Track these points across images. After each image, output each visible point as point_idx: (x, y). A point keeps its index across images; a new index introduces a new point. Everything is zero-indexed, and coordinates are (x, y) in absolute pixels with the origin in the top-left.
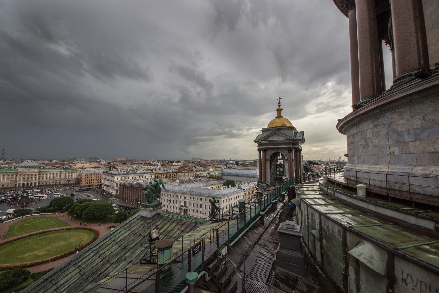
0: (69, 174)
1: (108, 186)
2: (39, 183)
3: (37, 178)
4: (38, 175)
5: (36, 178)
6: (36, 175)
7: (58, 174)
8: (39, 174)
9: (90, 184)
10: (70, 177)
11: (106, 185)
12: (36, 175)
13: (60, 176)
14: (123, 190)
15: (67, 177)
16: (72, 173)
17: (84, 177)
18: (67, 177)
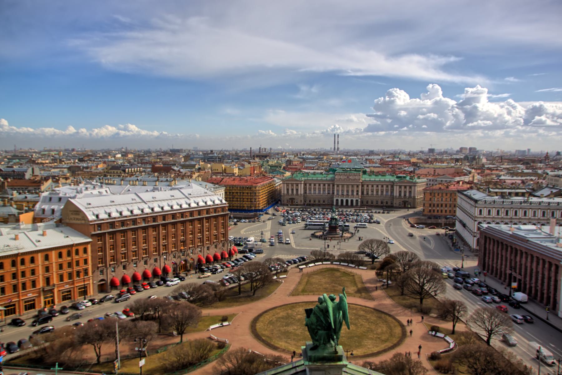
0: (405, 187)
1: (464, 225)
2: (362, 202)
3: (360, 194)
4: (360, 187)
5: (357, 191)
7: (390, 187)
9: (436, 213)
10: (407, 195)
11: (461, 222)
12: (358, 186)
14: (485, 244)
15: (403, 194)
16: (410, 187)
18: (403, 194)
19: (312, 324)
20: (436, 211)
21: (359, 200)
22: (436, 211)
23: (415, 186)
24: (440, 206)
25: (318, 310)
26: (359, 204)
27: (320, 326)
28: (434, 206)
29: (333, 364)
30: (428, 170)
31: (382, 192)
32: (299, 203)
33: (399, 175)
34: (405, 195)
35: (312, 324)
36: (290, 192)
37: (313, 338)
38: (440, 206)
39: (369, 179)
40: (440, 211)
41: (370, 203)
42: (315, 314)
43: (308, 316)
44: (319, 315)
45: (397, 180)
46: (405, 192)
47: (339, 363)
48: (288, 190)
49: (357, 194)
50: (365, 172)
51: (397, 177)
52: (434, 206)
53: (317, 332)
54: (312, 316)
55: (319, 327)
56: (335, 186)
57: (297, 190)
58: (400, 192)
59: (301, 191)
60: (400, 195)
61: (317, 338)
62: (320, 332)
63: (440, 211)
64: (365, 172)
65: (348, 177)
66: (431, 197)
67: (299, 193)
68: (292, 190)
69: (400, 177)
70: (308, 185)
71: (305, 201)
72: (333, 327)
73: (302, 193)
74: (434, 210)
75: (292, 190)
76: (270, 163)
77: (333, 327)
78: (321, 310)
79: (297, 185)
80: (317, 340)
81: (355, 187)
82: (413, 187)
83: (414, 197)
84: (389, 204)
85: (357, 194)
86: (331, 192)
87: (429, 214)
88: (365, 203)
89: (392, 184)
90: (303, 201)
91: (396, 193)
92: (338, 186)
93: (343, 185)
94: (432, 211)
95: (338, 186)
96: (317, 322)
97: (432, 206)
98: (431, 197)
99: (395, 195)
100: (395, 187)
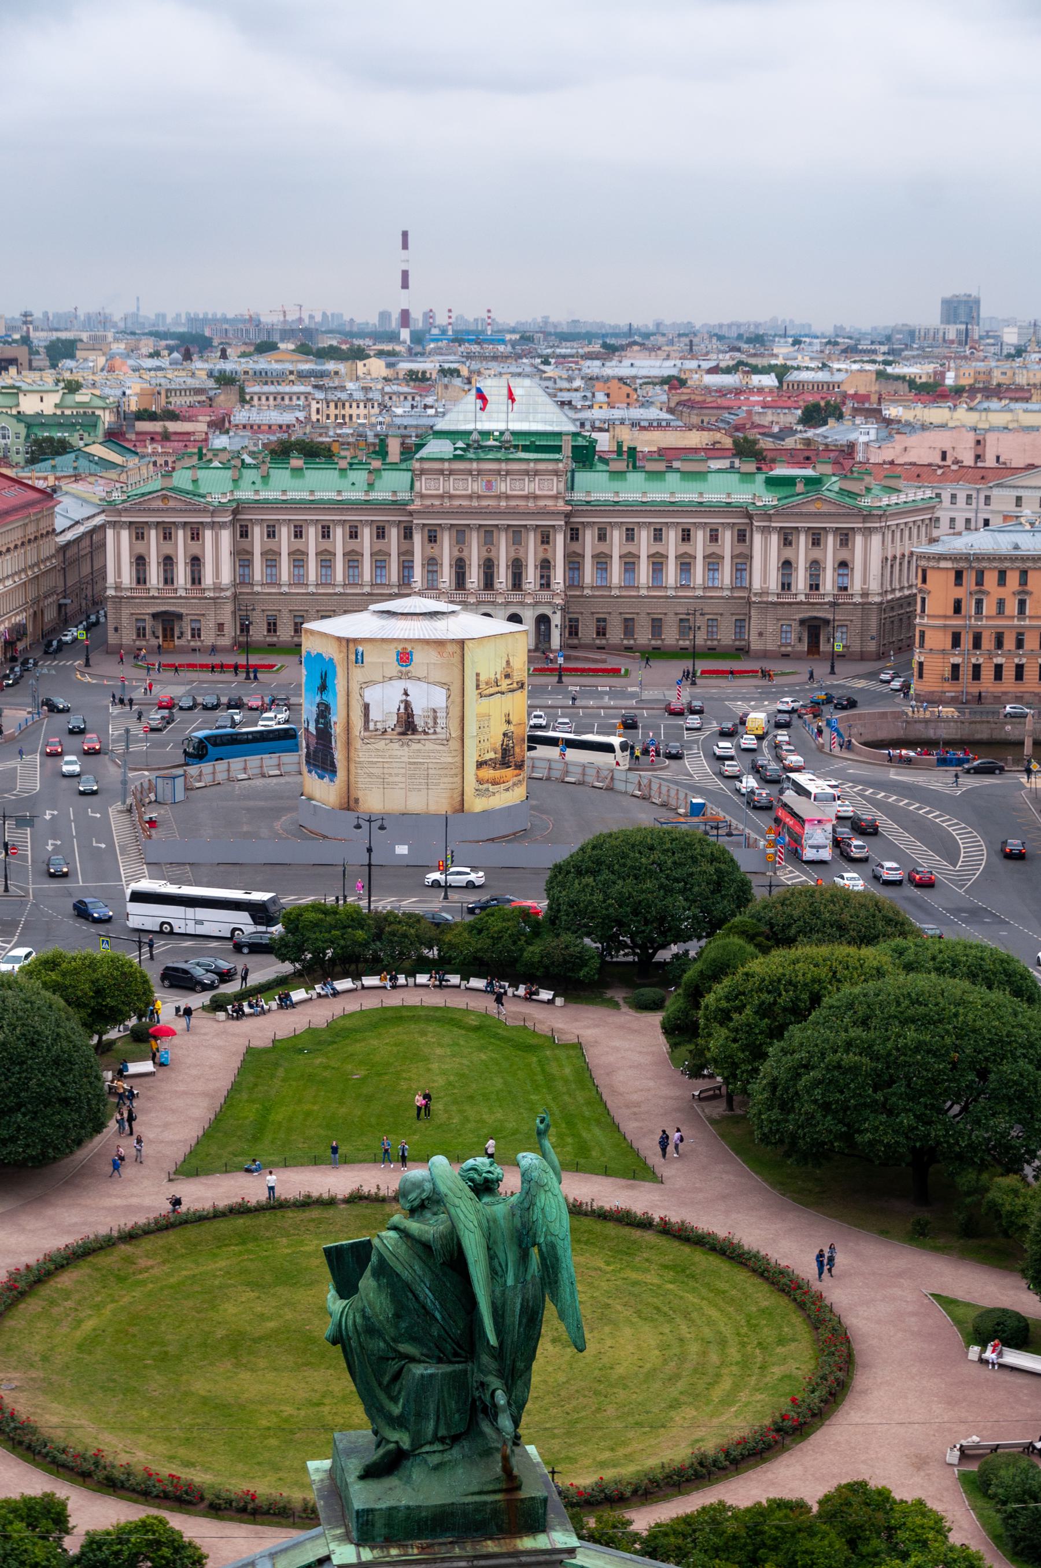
2: (572, 629)
3: (558, 577)
4: (560, 539)
5: (545, 565)
6: (546, 539)
7: (727, 538)
8: (574, 534)
10: (829, 583)
12: (546, 539)
13: (743, 562)
15: (801, 581)
16: (845, 538)
17: (940, 594)
18: (801, 581)
19: (371, 1330)
20: (988, 673)
21: (556, 619)
22: (988, 673)
23: (868, 532)
24: (1009, 643)
25: (402, 1250)
26: (556, 641)
27: (414, 1339)
28: (977, 644)
29: (491, 1546)
30: (942, 440)
31: (685, 564)
32: (208, 638)
33: (781, 471)
34: (815, 587)
35: (371, 1330)
36: (154, 574)
37: (374, 1409)
38: (1009, 643)
39: (610, 497)
40: (1009, 673)
41: (615, 635)
42: (384, 1270)
43: (346, 1289)
44: (405, 1275)
45: (768, 499)
46: (815, 567)
47: (527, 1543)
48: (140, 561)
49: (546, 584)
50: (585, 456)
51: (773, 482)
52: (977, 644)
53: (397, 1376)
54: (367, 1283)
55: (405, 1348)
56: (417, 538)
57: (196, 561)
58: (787, 565)
59: (220, 569)
60: (786, 586)
61: (396, 1410)
62: (419, 1370)
63: (1009, 673)
64: (585, 456)
65: (489, 485)
66: (960, 593)
67: (208, 580)
68: (168, 561)
69: (789, 482)
70: (257, 533)
71: (245, 629)
72: (493, 1340)
73: (226, 578)
74: (977, 669)
75: (168, 561)
76: (29, 405)
77: (493, 1340)
78: (423, 1248)
79: (196, 536)
80: (398, 1422)
81: (532, 540)
82: (859, 540)
83: (865, 594)
84: (726, 636)
85: (546, 584)
86: (394, 578)
87: (951, 690)
88: (587, 632)
89: (745, 522)
90: (230, 630)
91: (764, 577)
92: (432, 538)
93: (460, 533)
94: (966, 673)
95: (432, 538)
96: (397, 1316)
97: (967, 641)
98: (960, 593)
99: (757, 585)
100: (757, 538)
